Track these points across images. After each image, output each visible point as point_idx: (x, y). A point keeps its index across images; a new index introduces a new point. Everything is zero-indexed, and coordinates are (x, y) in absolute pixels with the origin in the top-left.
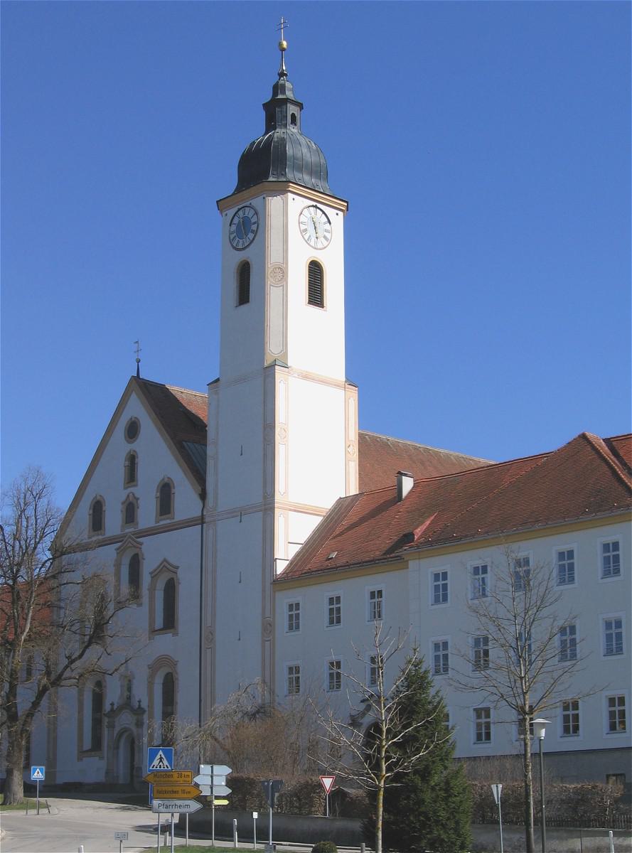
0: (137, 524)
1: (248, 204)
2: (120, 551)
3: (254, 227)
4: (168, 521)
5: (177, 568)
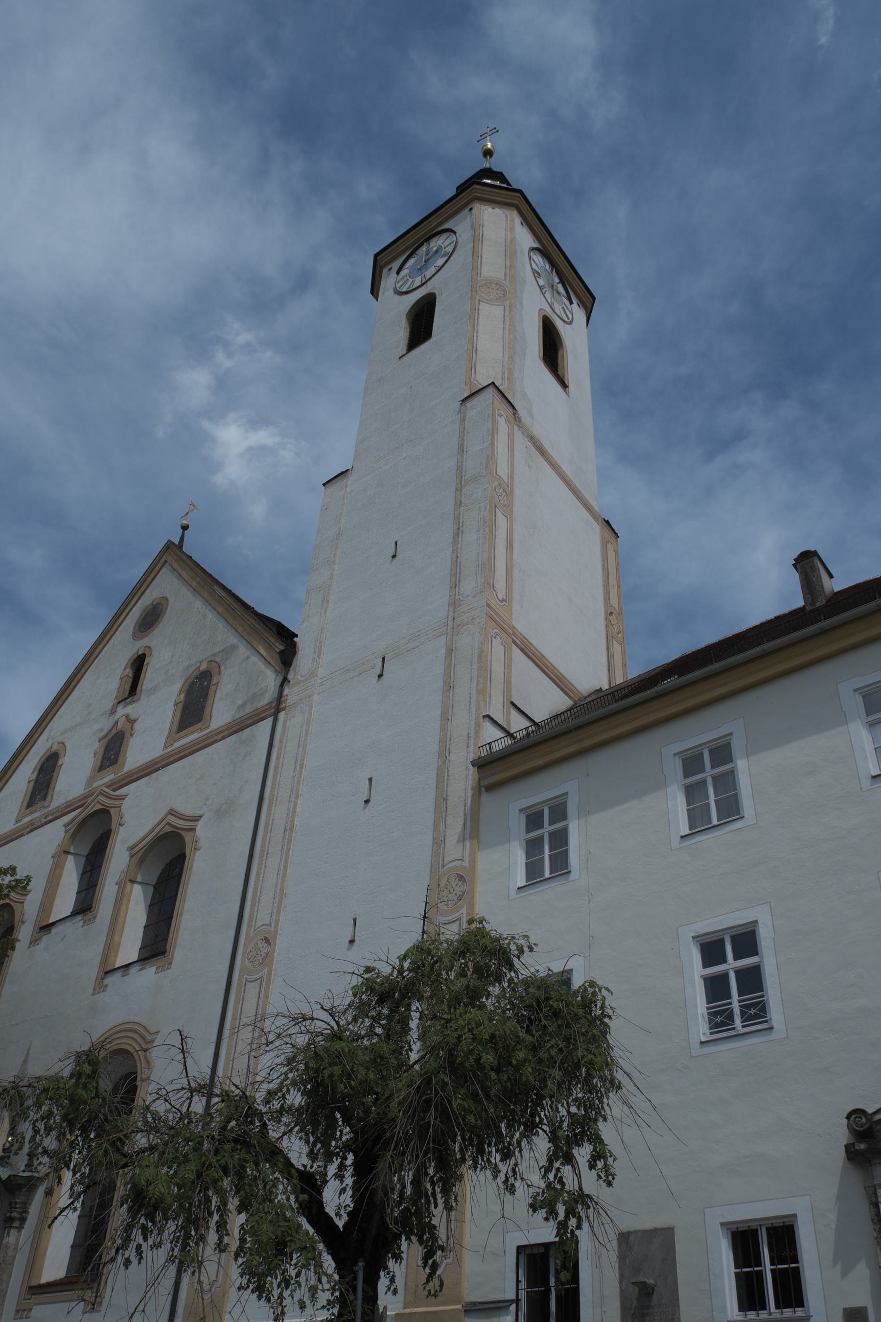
4: (195, 736)
5: (197, 819)
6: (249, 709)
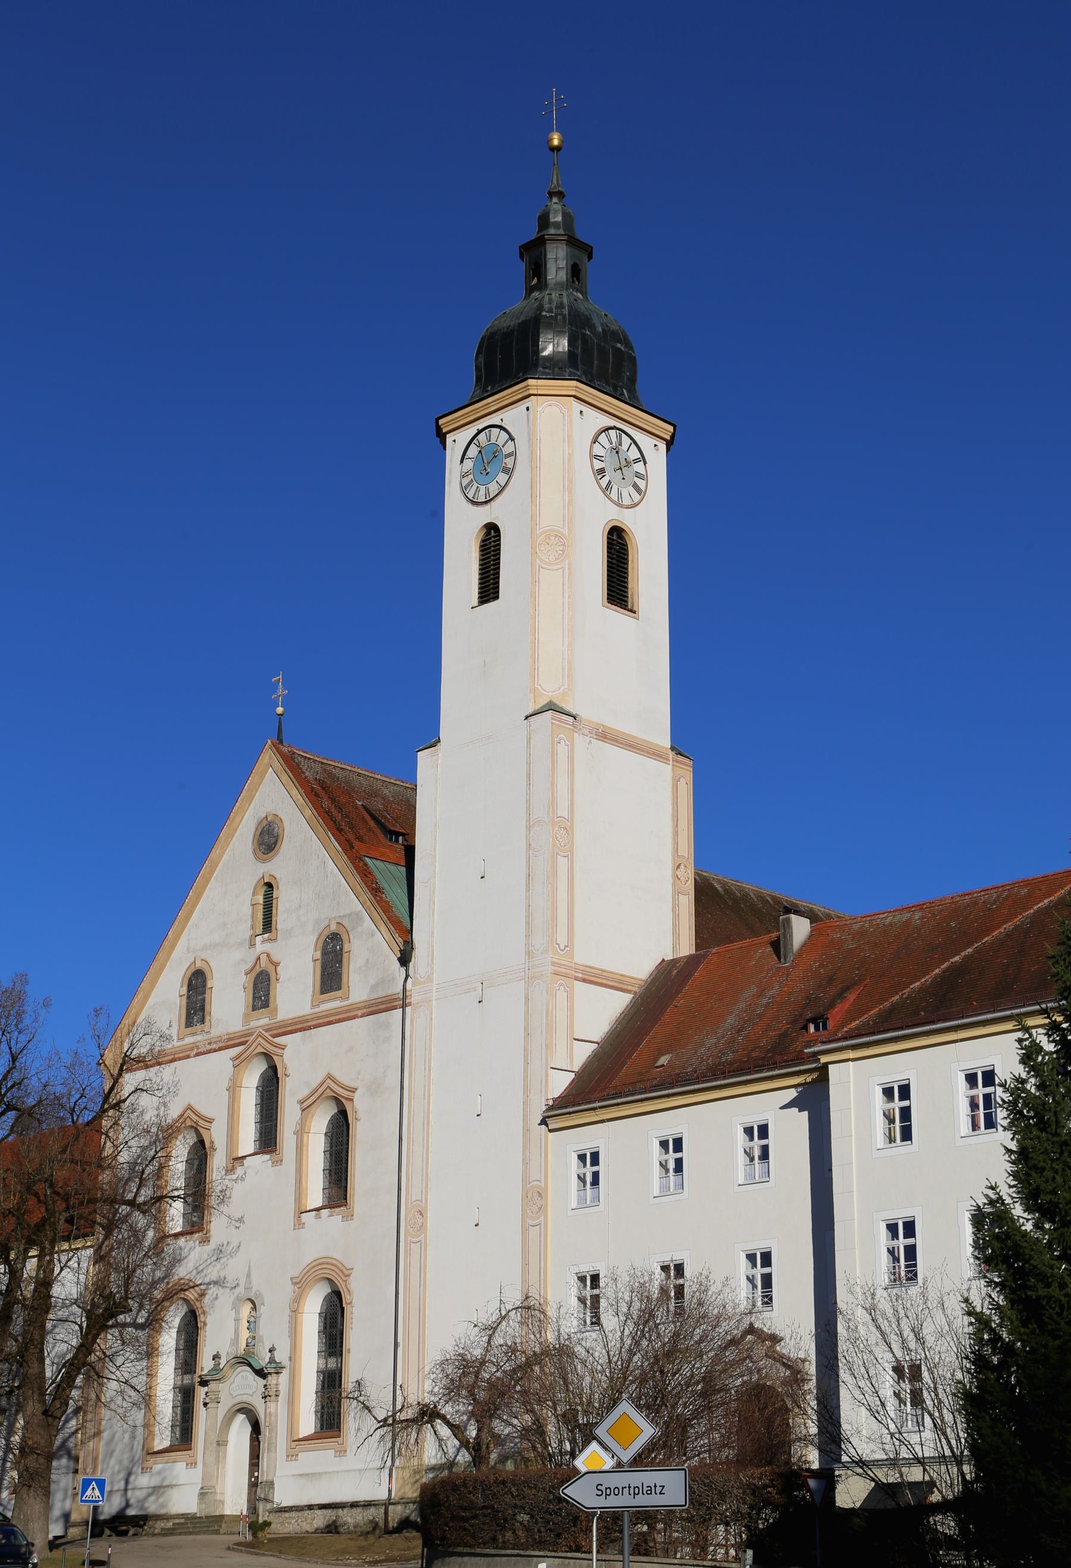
0: (276, 1009)
1: (494, 420)
2: (239, 1062)
3: (509, 462)
4: (337, 1004)
5: (353, 1090)
6: (381, 993)
